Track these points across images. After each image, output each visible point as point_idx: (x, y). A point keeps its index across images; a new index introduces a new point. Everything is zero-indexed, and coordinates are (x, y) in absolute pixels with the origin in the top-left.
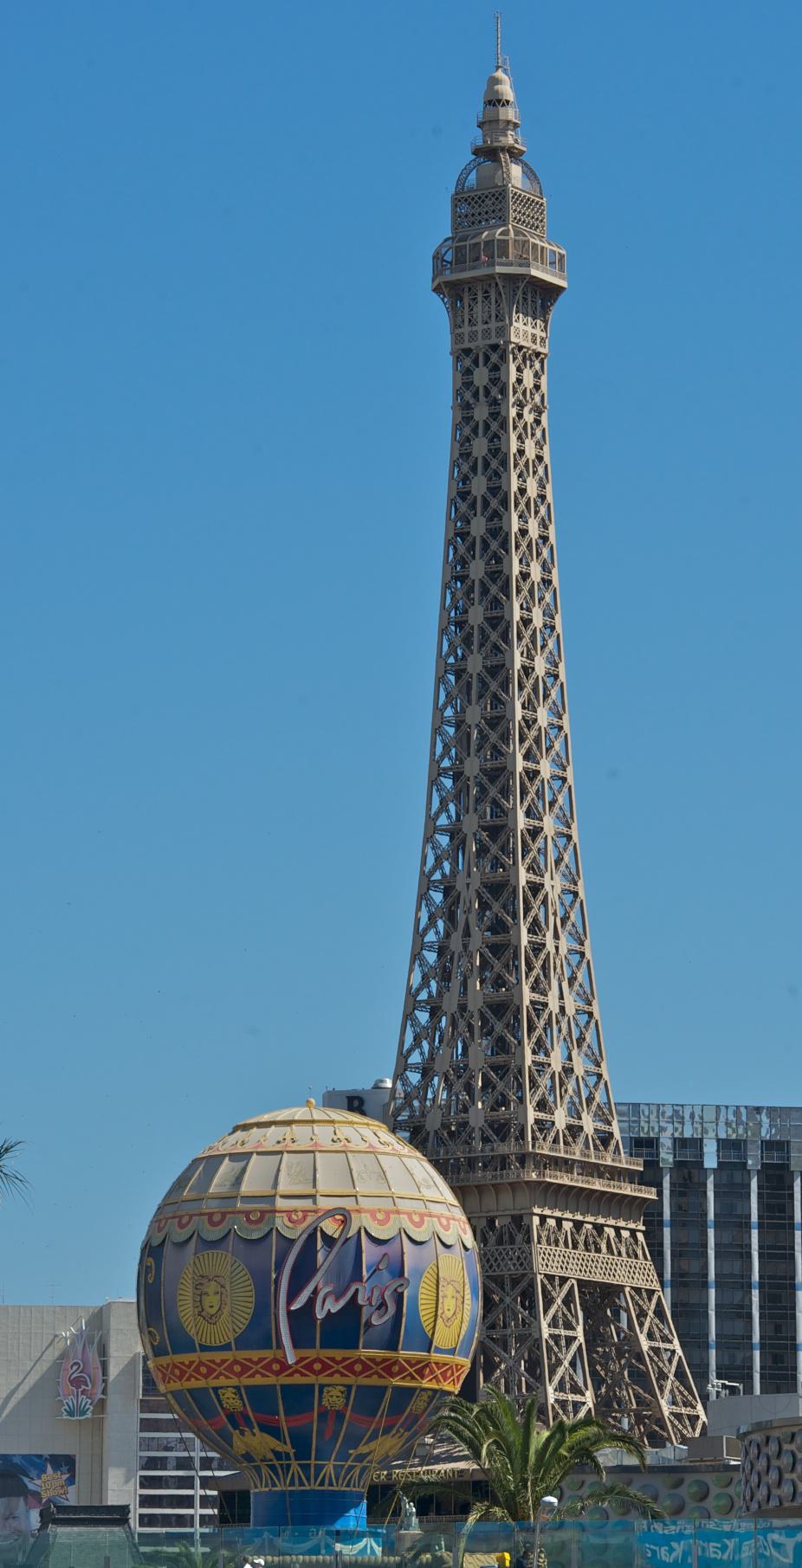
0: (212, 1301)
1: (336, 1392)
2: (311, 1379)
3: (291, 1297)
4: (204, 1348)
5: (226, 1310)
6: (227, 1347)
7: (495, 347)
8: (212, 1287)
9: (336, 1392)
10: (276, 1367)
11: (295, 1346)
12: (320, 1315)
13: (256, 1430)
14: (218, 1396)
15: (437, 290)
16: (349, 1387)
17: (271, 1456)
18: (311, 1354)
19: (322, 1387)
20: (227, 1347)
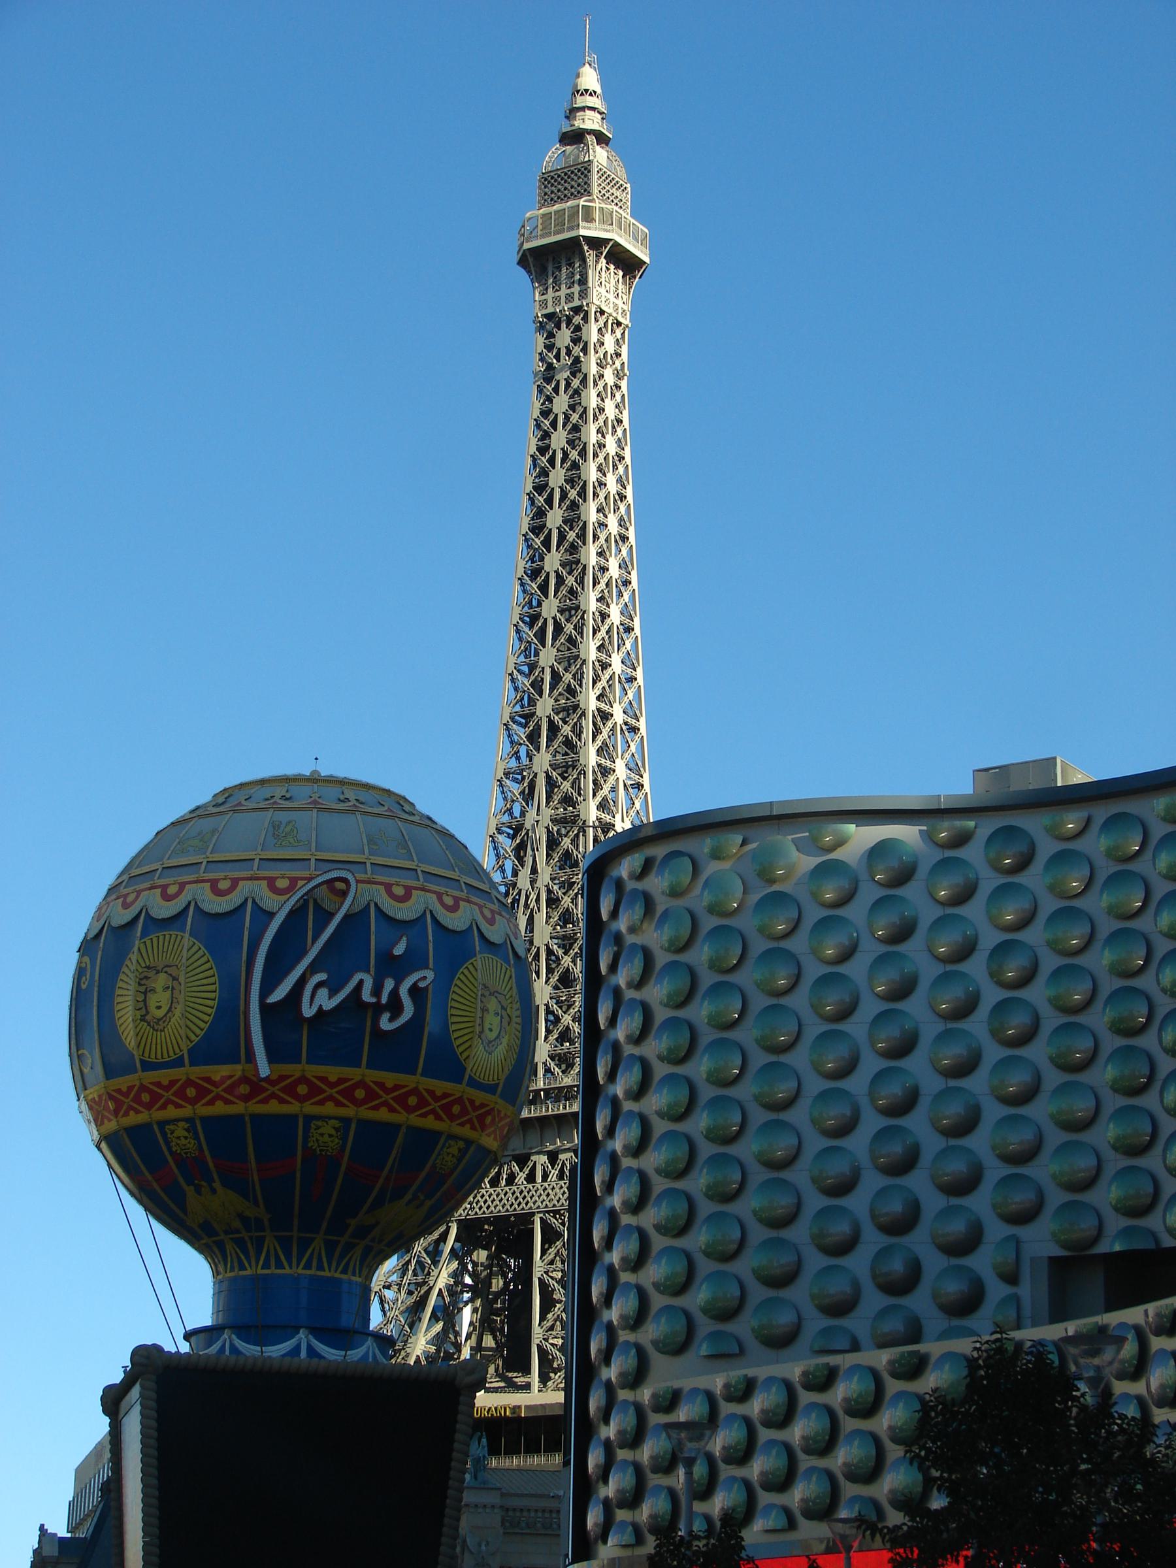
0: (159, 999)
1: (327, 1129)
2: (293, 1108)
3: (268, 987)
4: (147, 1066)
5: (178, 1012)
6: (178, 1062)
7: (577, 310)
8: (161, 980)
9: (327, 1129)
10: (244, 1089)
11: (272, 1058)
12: (308, 1012)
13: (217, 1185)
14: (164, 1134)
15: (523, 262)
16: (346, 1121)
17: (237, 1224)
18: (293, 1070)
19: (309, 1118)
20: (178, 1062)
